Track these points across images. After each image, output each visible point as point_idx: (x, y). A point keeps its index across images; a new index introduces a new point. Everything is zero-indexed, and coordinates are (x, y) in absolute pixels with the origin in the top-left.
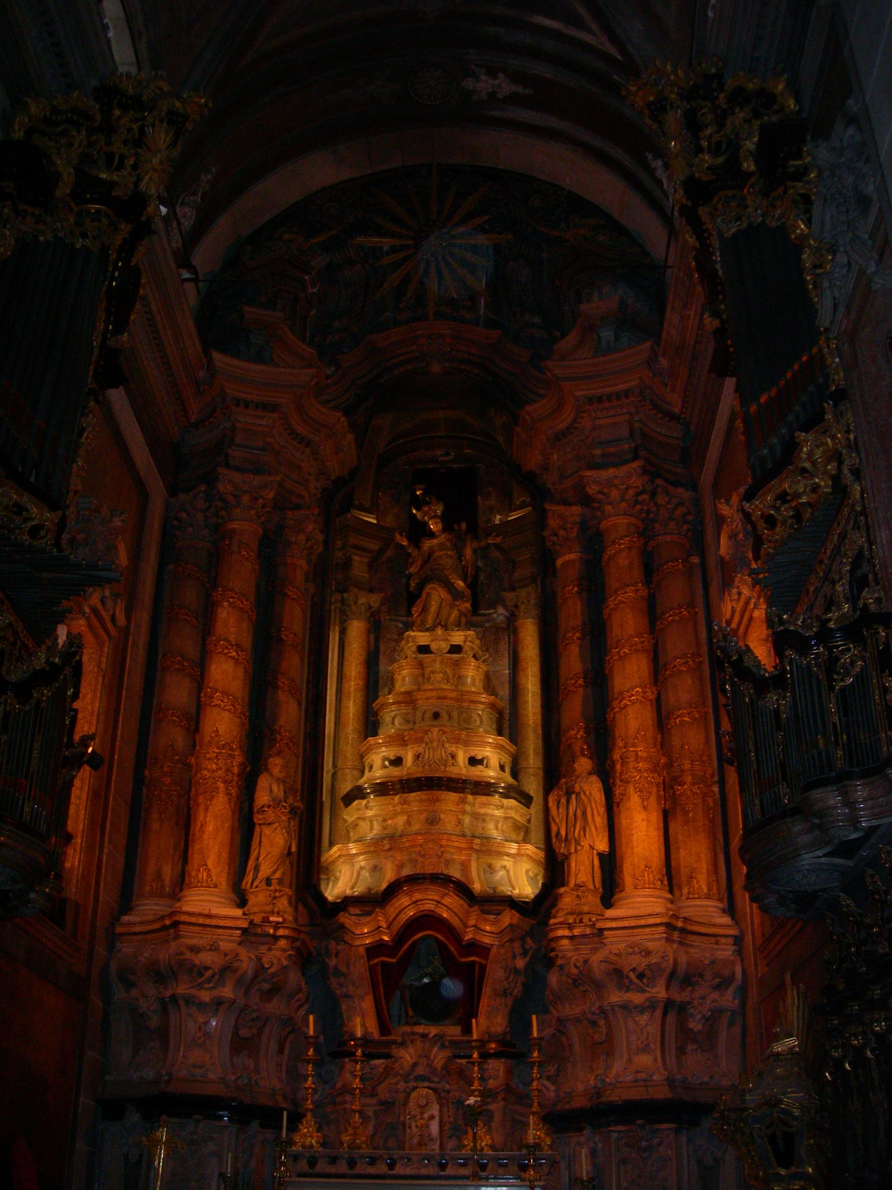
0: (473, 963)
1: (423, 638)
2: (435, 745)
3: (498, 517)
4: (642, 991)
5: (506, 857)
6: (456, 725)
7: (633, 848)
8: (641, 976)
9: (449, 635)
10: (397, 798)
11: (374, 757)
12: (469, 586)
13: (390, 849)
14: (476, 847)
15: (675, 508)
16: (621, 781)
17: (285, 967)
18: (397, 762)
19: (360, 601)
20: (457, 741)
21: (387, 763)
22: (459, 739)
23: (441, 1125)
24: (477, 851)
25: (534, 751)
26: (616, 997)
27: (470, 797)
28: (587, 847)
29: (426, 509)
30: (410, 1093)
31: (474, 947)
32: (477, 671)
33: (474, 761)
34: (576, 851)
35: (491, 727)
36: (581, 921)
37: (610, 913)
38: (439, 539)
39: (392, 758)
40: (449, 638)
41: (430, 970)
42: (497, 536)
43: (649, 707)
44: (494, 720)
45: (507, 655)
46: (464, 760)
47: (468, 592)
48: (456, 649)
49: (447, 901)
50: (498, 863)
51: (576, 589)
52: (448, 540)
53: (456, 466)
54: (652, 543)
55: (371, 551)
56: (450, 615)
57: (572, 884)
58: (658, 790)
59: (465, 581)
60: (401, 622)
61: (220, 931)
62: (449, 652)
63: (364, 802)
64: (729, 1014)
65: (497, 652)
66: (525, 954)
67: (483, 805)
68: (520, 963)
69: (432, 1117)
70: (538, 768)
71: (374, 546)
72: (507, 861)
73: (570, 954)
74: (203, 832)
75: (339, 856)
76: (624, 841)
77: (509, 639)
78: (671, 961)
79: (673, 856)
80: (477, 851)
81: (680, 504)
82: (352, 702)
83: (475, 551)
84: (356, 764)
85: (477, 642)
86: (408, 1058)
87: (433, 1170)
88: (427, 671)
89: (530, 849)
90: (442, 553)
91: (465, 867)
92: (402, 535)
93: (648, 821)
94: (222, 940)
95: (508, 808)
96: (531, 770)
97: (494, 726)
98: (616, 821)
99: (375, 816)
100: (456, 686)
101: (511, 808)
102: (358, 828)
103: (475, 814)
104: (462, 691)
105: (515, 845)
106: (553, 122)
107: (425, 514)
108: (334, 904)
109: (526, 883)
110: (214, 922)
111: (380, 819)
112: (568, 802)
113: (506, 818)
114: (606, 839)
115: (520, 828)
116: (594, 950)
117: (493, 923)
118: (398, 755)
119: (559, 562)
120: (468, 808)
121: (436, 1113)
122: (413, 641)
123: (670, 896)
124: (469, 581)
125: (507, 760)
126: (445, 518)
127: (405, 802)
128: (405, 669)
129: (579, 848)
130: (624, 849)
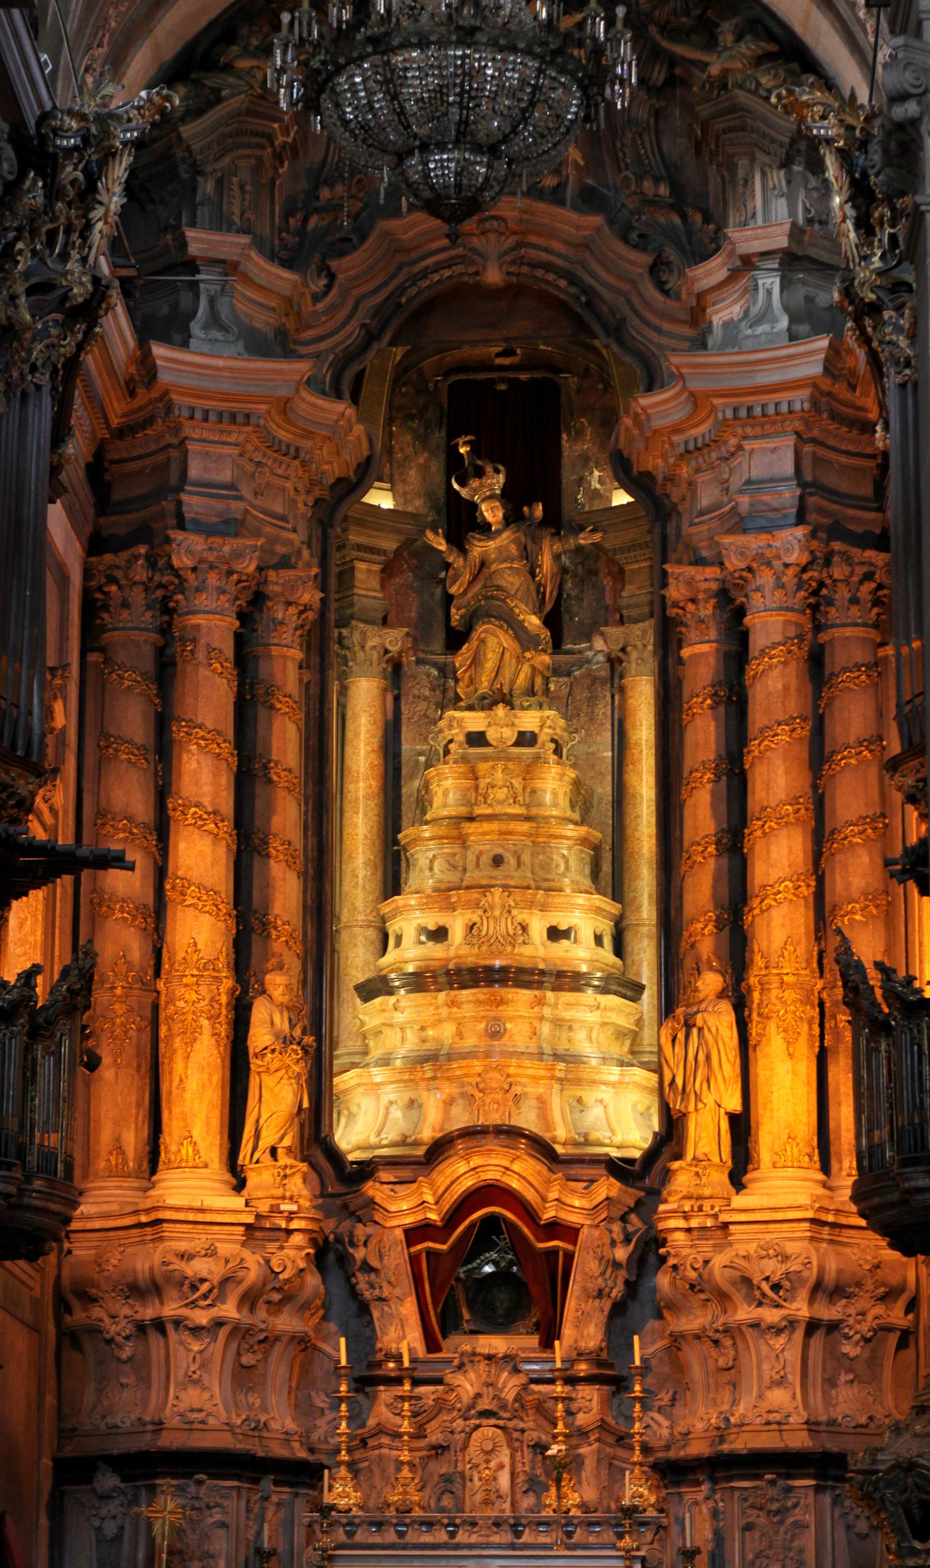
0: (554, 1252)
1: (475, 721)
2: (497, 913)
3: (596, 473)
4: (778, 1306)
5: (603, 1087)
6: (529, 875)
7: (772, 1110)
8: (776, 1287)
9: (515, 716)
10: (442, 996)
11: (403, 924)
13: (434, 1078)
14: (559, 1075)
15: (861, 582)
16: (759, 1015)
17: (302, 1270)
18: (439, 934)
19: (370, 644)
20: (530, 905)
21: (423, 938)
23: (513, 1475)
24: (561, 1080)
25: (650, 896)
26: (744, 1313)
27: (550, 995)
28: (711, 1104)
29: (475, 483)
30: (470, 1434)
31: (556, 1229)
33: (555, 934)
34: (696, 1110)
36: (700, 1209)
37: (739, 1201)
39: (432, 927)
40: (516, 721)
41: (494, 1255)
43: (802, 910)
44: (588, 860)
45: (609, 726)
47: (546, 634)
48: (526, 739)
49: (516, 1167)
50: (590, 1096)
51: (709, 701)
52: (514, 541)
53: (524, 377)
54: (823, 637)
55: (385, 552)
57: (689, 1156)
58: (810, 1029)
60: (434, 665)
61: (216, 1228)
62: (517, 744)
63: (392, 1000)
64: (898, 1334)
65: (592, 720)
66: (627, 1240)
68: (621, 1254)
69: (501, 1466)
71: (390, 544)
73: (685, 1252)
74: (184, 1090)
75: (358, 1085)
76: (760, 1100)
77: (613, 697)
78: (815, 1270)
79: (832, 1113)
80: (561, 1080)
81: (868, 576)
82: (361, 815)
83: (557, 557)
86: (469, 1387)
87: (508, 1537)
88: (483, 783)
91: (543, 1105)
92: (437, 534)
93: (795, 1073)
94: (219, 1240)
96: (645, 929)
97: (587, 871)
98: (752, 1070)
100: (528, 807)
101: (612, 1009)
105: (617, 1070)
107: (475, 491)
109: (633, 1124)
110: (209, 1218)
111: (417, 1027)
112: (687, 1037)
113: (604, 1024)
114: (738, 1095)
116: (718, 1248)
117: (583, 1196)
118: (441, 923)
119: (686, 653)
120: (547, 1011)
121: (506, 1460)
122: (460, 726)
123: (821, 1177)
124: (548, 607)
125: (606, 927)
127: (453, 1003)
129: (700, 1105)
130: (760, 1111)
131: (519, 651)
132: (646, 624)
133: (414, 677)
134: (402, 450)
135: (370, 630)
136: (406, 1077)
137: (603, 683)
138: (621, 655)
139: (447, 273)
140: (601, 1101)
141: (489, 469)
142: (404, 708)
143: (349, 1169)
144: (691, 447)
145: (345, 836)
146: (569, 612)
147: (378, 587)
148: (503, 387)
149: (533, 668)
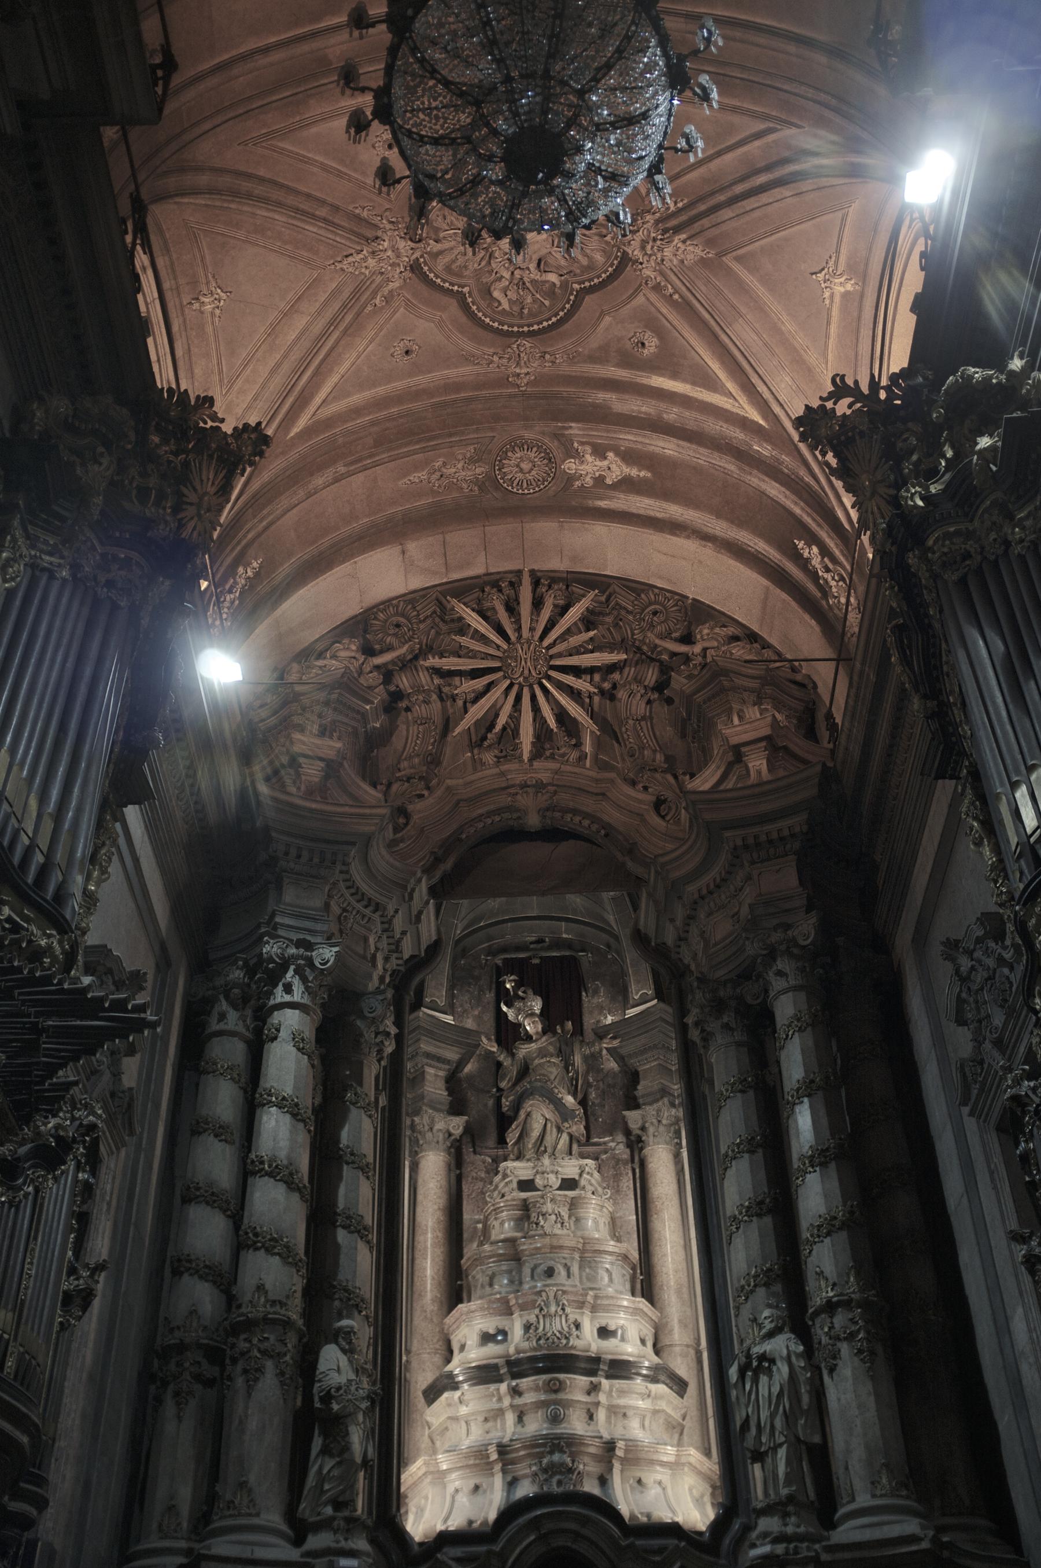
5: (658, 1468)
10: (503, 1387)
12: (580, 1103)
19: (437, 1127)
20: (581, 1305)
22: (583, 1303)
24: (624, 1461)
27: (605, 1383)
29: (518, 1004)
32: (601, 1210)
33: (604, 1332)
35: (624, 1285)
38: (539, 1043)
42: (614, 1038)
44: (628, 1277)
46: (592, 1332)
48: (569, 1184)
52: (551, 1044)
55: (448, 1062)
56: (558, 1140)
59: (575, 1096)
62: (560, 1188)
63: (457, 1394)
65: (618, 1191)
67: (622, 1393)
70: (688, 1346)
71: (452, 1054)
72: (662, 1473)
83: (585, 1059)
84: (438, 1346)
85: (596, 1175)
89: (694, 1455)
90: (544, 1060)
92: (489, 1039)
95: (657, 1397)
96: (677, 1349)
97: (628, 1286)
99: (473, 1414)
102: (448, 1434)
103: (613, 1406)
104: (583, 1238)
106: (675, 511)
107: (519, 1011)
108: (421, 1544)
109: (691, 1505)
111: (481, 1418)
113: (655, 1412)
115: (674, 1428)
124: (580, 1096)
126: (544, 1014)
127: (516, 1392)
128: (502, 1211)
131: (559, 1121)
132: (660, 1103)
133: (473, 1163)
134: (462, 1006)
135: (438, 1116)
136: (471, 1462)
137: (625, 1163)
138: (639, 1132)
139: (497, 818)
140: (660, 1483)
141: (530, 992)
142: (465, 1188)
143: (416, 1548)
144: (704, 892)
145: (416, 1279)
146: (594, 1115)
147: (443, 1088)
148: (536, 961)
149: (571, 1136)
